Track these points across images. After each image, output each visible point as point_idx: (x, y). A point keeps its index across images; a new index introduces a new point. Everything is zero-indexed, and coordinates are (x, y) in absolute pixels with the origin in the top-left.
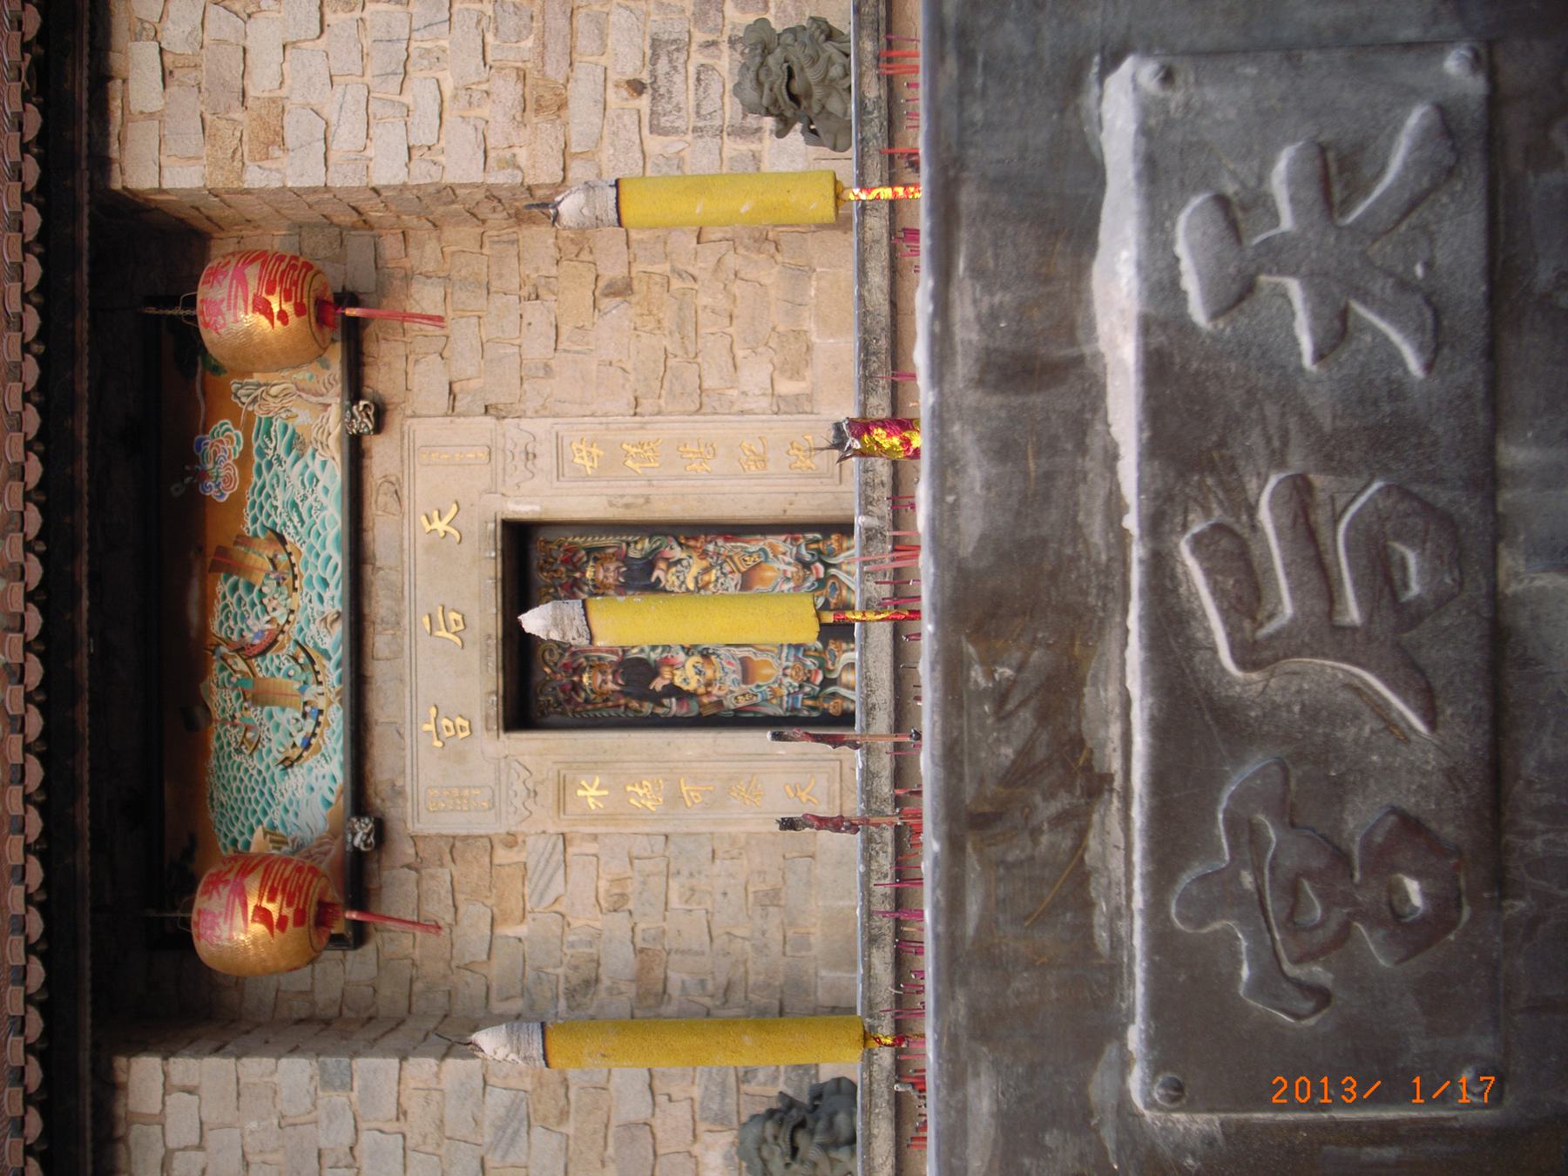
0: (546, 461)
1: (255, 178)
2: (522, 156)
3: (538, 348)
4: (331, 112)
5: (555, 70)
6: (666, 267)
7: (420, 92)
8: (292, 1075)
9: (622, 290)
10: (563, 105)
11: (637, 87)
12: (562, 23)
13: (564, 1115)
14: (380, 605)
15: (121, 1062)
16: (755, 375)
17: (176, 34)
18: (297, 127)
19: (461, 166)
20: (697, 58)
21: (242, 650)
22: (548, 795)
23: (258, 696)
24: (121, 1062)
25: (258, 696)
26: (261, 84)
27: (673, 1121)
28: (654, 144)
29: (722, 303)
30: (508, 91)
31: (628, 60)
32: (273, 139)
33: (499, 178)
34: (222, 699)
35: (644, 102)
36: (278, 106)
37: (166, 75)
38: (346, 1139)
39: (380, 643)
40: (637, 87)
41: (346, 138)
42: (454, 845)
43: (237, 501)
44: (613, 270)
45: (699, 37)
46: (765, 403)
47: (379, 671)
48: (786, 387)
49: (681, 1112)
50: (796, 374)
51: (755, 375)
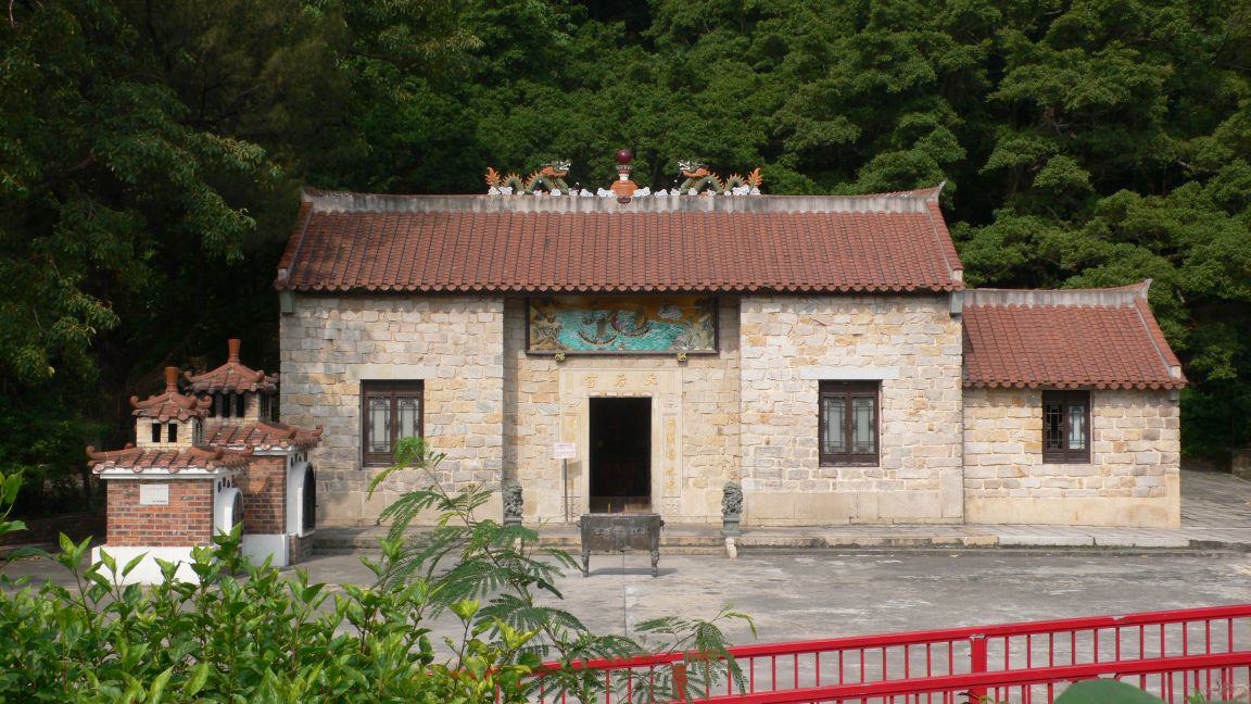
0: (669, 410)
1: (743, 338)
2: (750, 412)
3: (702, 407)
4: (762, 359)
5: (772, 421)
6: (727, 445)
7: (767, 384)
8: (499, 348)
9: (720, 432)
10: (763, 423)
11: (768, 443)
12: (786, 423)
13: (487, 422)
14: (627, 361)
15: (502, 300)
16: (694, 472)
17: (783, 317)
18: (757, 350)
19: (746, 395)
20: (776, 460)
21: (614, 319)
22: (571, 411)
23: (602, 323)
24: (502, 300)
25: (602, 323)
26: (770, 339)
27: (485, 451)
28: (752, 449)
29: (715, 463)
30: (767, 408)
31: (776, 438)
32: (754, 343)
33: (743, 405)
34: (599, 315)
35: (764, 445)
36: (764, 344)
37: (773, 313)
38: (481, 363)
39: (616, 361)
40: (768, 443)
41: (754, 363)
42: (555, 382)
43: (658, 319)
44: (726, 430)
45: (782, 461)
46: (686, 475)
47: (608, 361)
48: (691, 481)
49: (487, 455)
50: (695, 484)
51: (694, 472)
